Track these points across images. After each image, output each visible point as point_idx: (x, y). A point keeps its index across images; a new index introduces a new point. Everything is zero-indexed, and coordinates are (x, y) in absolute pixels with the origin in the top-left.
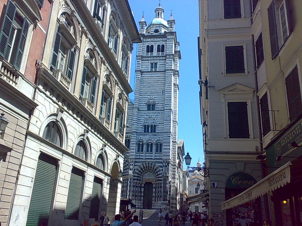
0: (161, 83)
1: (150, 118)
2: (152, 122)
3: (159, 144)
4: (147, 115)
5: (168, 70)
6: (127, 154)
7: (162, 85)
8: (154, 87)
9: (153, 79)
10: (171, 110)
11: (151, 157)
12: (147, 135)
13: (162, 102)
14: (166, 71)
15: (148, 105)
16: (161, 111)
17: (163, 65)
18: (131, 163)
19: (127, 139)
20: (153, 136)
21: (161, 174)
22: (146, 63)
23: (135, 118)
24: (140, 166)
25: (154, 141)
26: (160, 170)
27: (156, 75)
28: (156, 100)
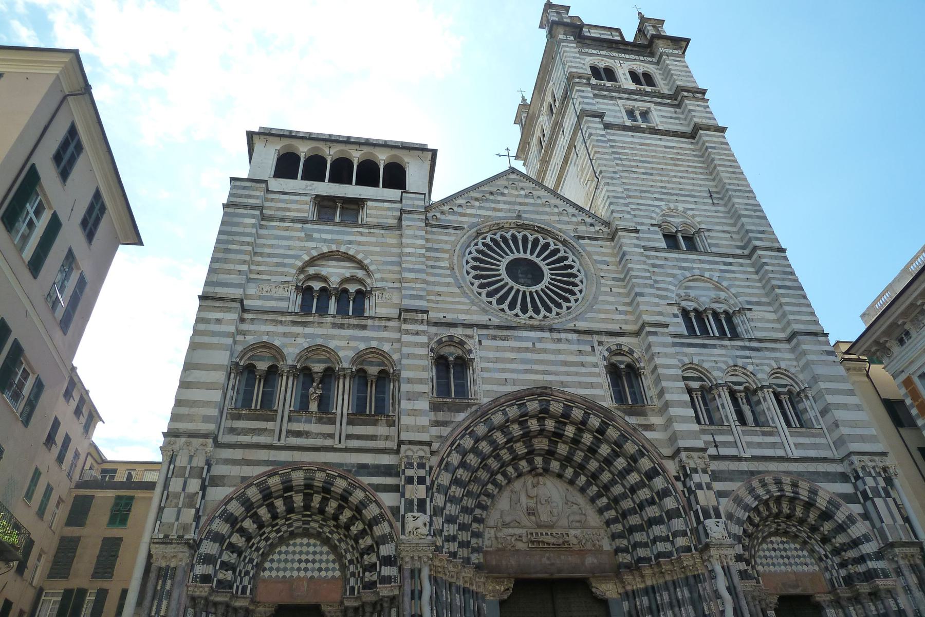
0: (689, 166)
1: (696, 280)
2: (714, 296)
3: (785, 390)
4: (681, 268)
5: (708, 128)
6: (649, 435)
7: (695, 173)
8: (668, 176)
9: (655, 151)
10: (784, 251)
11: (780, 453)
12: (714, 346)
13: (726, 228)
14: (701, 132)
15: (664, 235)
16: (734, 256)
17: (672, 118)
18: (696, 478)
19: (622, 362)
20: (747, 353)
21: (866, 538)
22: (607, 104)
23: (638, 266)
24: (738, 501)
25: (760, 376)
26: (851, 519)
27: (662, 143)
28: (698, 219)
